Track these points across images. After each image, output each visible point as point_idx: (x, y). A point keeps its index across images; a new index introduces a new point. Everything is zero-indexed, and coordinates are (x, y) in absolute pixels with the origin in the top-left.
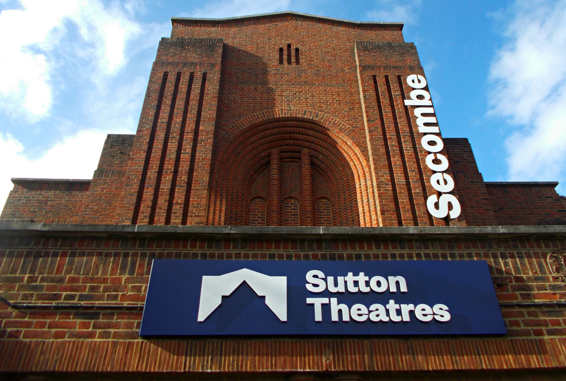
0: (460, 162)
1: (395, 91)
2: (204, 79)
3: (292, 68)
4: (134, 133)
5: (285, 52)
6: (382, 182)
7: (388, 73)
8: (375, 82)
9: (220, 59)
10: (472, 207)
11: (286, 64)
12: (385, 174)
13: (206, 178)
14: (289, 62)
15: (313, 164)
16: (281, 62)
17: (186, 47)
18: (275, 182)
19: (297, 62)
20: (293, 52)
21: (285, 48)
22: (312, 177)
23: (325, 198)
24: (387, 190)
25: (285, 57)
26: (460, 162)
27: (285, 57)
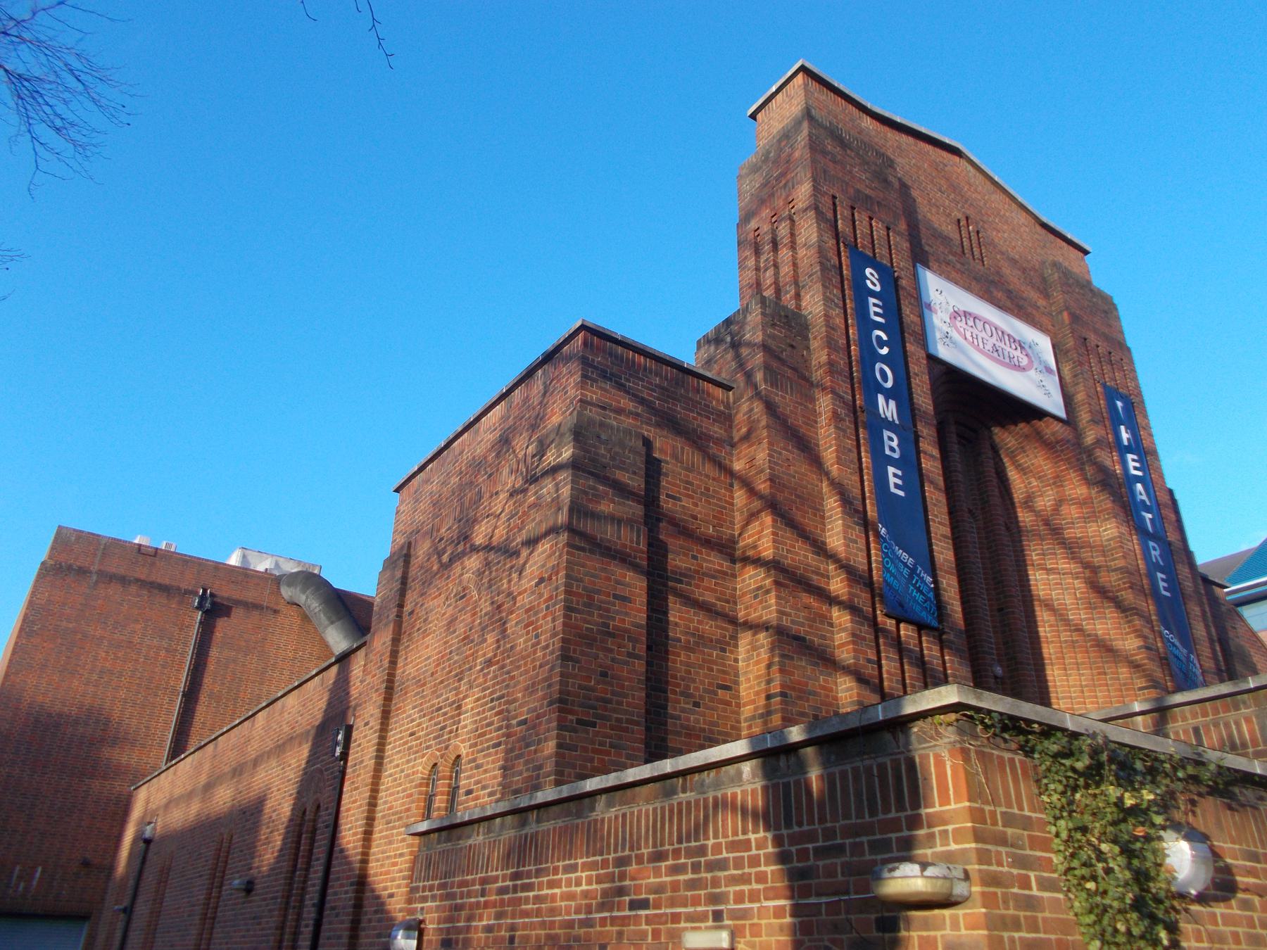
21: (963, 223)
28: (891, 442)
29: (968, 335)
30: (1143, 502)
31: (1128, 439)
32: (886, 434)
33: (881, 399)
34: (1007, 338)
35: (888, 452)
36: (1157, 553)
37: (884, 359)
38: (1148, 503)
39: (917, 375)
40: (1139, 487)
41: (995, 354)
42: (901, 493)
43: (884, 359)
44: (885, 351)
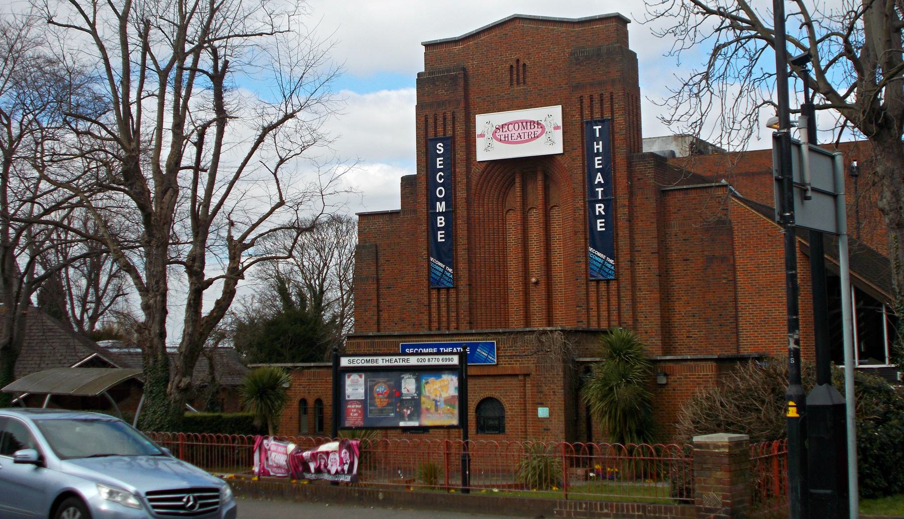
0: (642, 179)
1: (597, 113)
2: (454, 118)
3: (520, 90)
4: (416, 173)
5: (515, 72)
6: (577, 207)
7: (593, 91)
8: (582, 102)
9: (462, 93)
10: (642, 221)
11: (515, 85)
12: (580, 200)
13: (465, 214)
14: (518, 83)
15: (547, 178)
16: (511, 80)
17: (437, 83)
18: (518, 199)
19: (524, 83)
20: (521, 68)
21: (515, 65)
22: (546, 189)
23: (557, 206)
24: (580, 215)
25: (515, 77)
26: (642, 179)
27: (515, 77)
28: (441, 221)
29: (503, 138)
30: (599, 182)
31: (598, 149)
32: (439, 218)
33: (438, 203)
34: (529, 124)
35: (439, 226)
36: (601, 210)
37: (441, 185)
38: (603, 182)
39: (460, 182)
40: (599, 174)
41: (519, 139)
42: (444, 240)
43: (441, 185)
44: (443, 180)
